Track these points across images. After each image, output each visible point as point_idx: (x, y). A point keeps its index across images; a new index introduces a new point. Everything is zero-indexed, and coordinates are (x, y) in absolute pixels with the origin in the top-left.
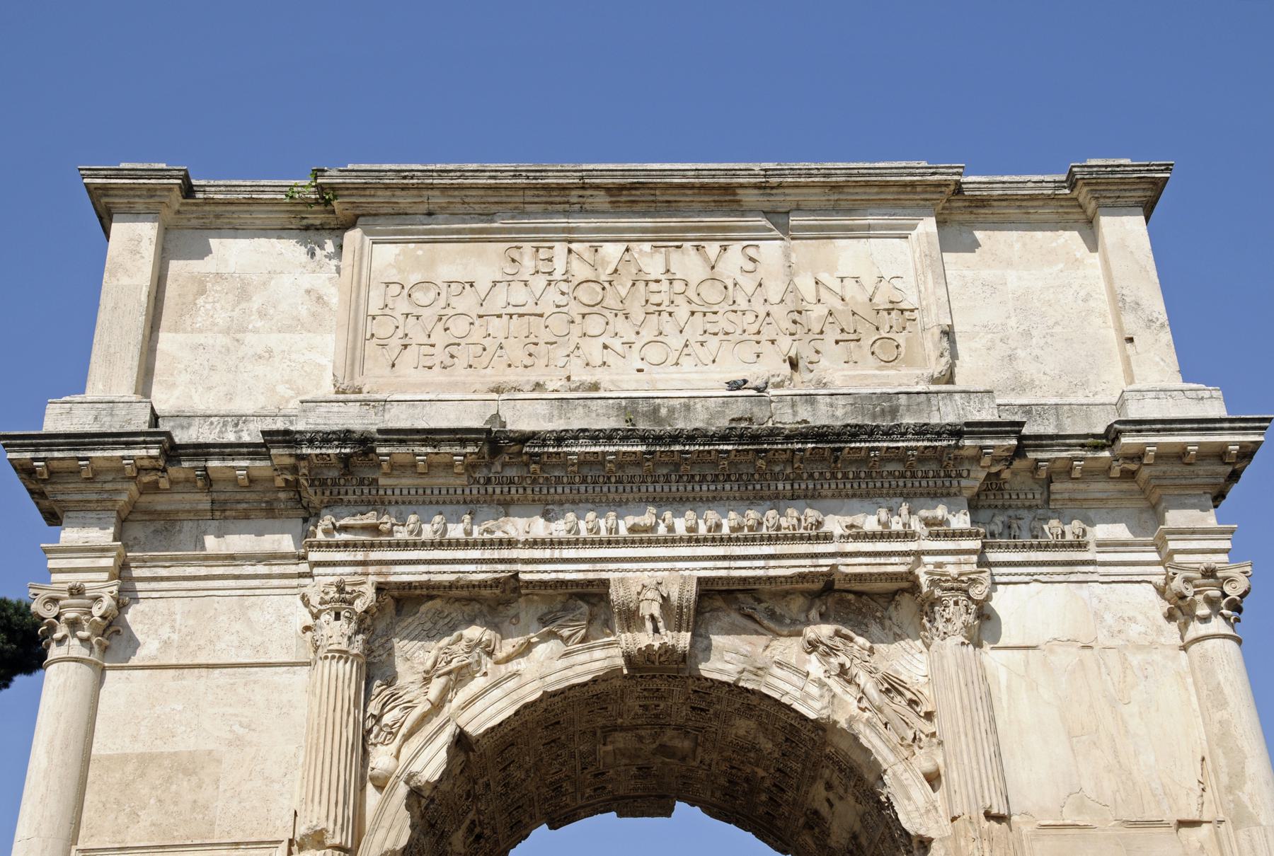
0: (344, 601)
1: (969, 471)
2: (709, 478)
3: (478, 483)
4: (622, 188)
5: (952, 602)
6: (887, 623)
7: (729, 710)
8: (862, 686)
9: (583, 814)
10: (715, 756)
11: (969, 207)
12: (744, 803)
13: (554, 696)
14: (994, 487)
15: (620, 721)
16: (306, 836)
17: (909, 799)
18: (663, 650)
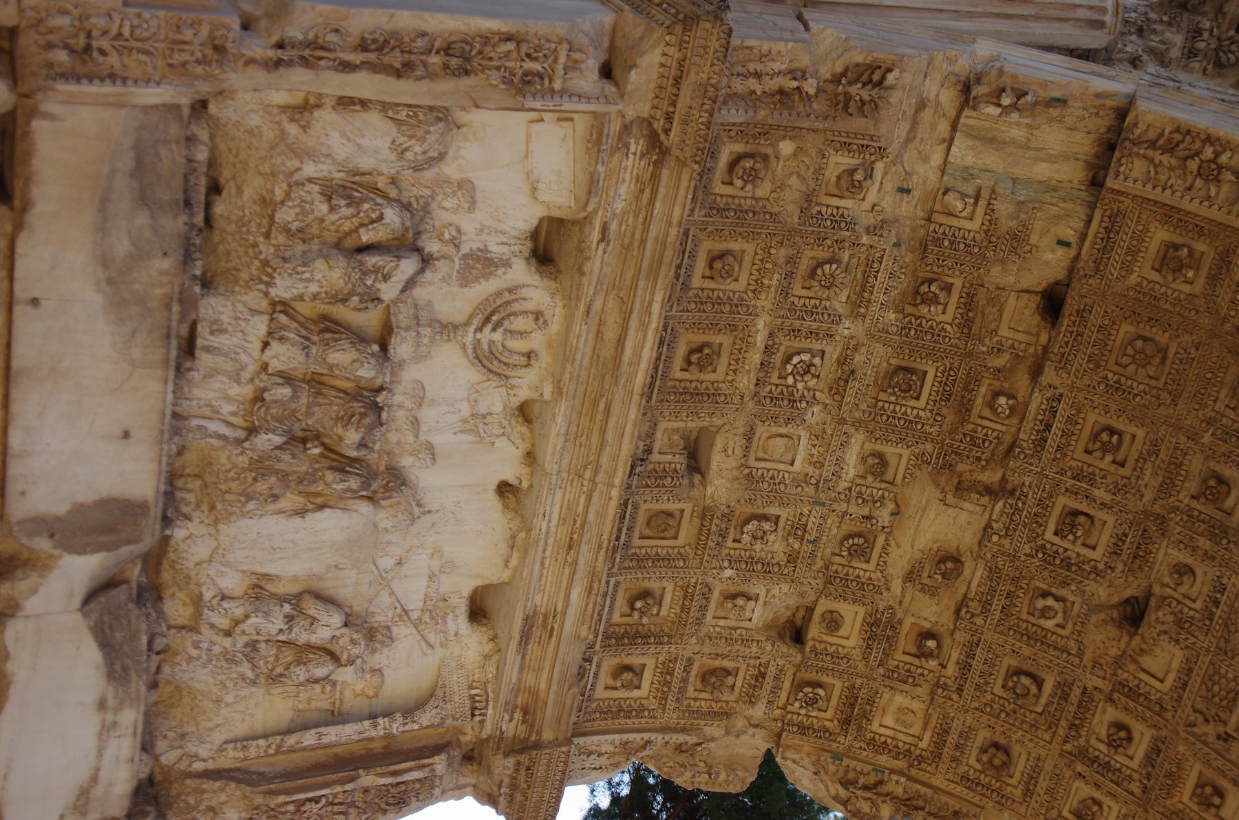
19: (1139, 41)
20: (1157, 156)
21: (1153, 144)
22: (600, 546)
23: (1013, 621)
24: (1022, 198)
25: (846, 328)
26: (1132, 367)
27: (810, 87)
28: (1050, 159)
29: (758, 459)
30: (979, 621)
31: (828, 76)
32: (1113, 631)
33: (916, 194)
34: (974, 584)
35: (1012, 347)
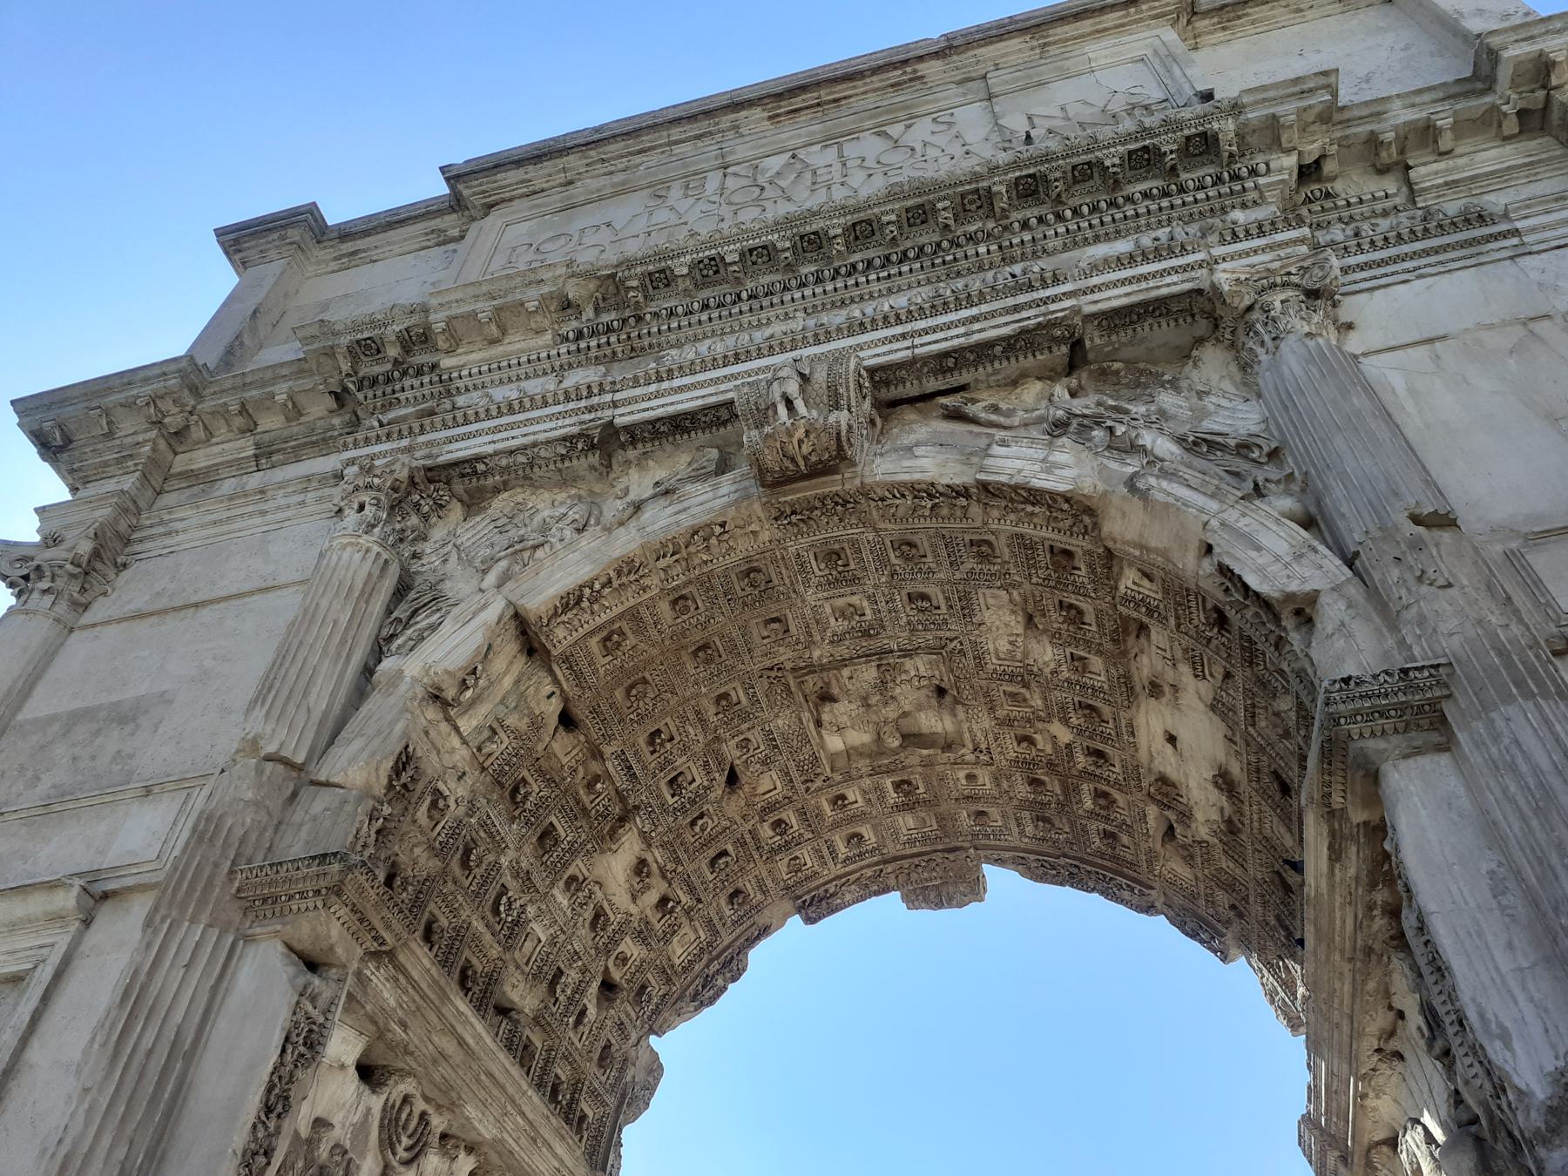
0: (369, 487)
1: (1267, 165)
2: (877, 262)
3: (567, 339)
4: (779, 96)
5: (1278, 304)
6: (1184, 384)
7: (958, 576)
8: (1149, 447)
9: (848, 897)
10: (986, 722)
11: (1219, 23)
12: (1070, 836)
13: (665, 556)
14: (1318, 194)
15: (817, 653)
16: (238, 751)
17: (1258, 548)
18: (800, 433)
19: (406, 544)
20: (564, 618)
21: (556, 614)
22: (548, 1117)
23: (691, 848)
24: (514, 704)
25: (504, 861)
26: (641, 703)
27: (387, 810)
28: (505, 673)
29: (527, 964)
30: (680, 869)
31: (383, 791)
32: (734, 797)
33: (467, 769)
34: (660, 860)
35: (577, 761)
